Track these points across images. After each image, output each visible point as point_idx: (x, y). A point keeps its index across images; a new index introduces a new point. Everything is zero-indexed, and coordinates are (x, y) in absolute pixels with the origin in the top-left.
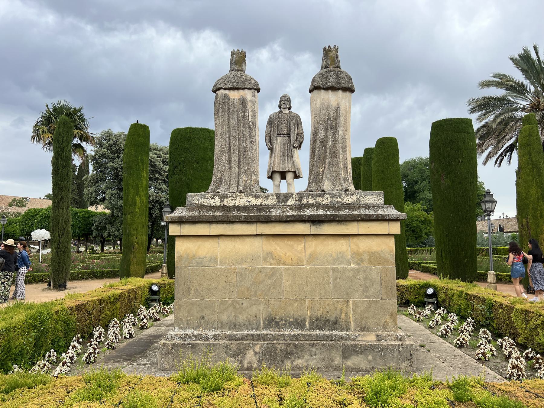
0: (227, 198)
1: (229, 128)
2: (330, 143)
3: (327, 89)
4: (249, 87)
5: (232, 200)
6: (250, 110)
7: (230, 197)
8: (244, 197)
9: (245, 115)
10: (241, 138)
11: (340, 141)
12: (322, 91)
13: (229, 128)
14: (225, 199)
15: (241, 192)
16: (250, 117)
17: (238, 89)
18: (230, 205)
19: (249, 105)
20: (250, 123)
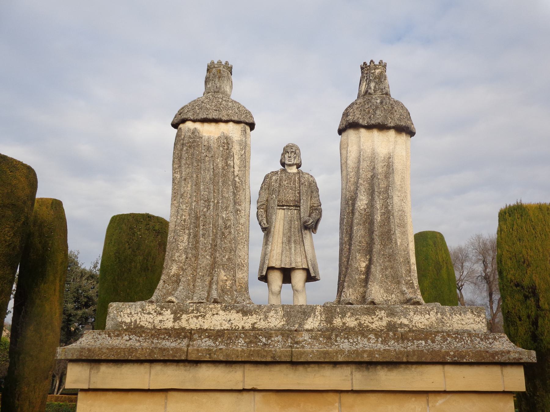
0: (187, 313)
1: (197, 184)
2: (378, 218)
3: (369, 127)
4: (236, 118)
5: (197, 317)
6: (236, 157)
7: (192, 312)
8: (221, 312)
9: (227, 165)
10: (218, 203)
11: (395, 214)
12: (363, 130)
13: (197, 184)
14: (184, 316)
15: (216, 302)
16: (237, 169)
17: (216, 121)
18: (193, 326)
19: (236, 149)
20: (237, 179)
